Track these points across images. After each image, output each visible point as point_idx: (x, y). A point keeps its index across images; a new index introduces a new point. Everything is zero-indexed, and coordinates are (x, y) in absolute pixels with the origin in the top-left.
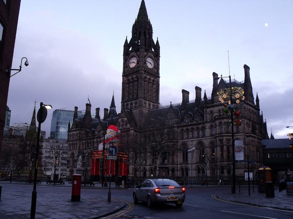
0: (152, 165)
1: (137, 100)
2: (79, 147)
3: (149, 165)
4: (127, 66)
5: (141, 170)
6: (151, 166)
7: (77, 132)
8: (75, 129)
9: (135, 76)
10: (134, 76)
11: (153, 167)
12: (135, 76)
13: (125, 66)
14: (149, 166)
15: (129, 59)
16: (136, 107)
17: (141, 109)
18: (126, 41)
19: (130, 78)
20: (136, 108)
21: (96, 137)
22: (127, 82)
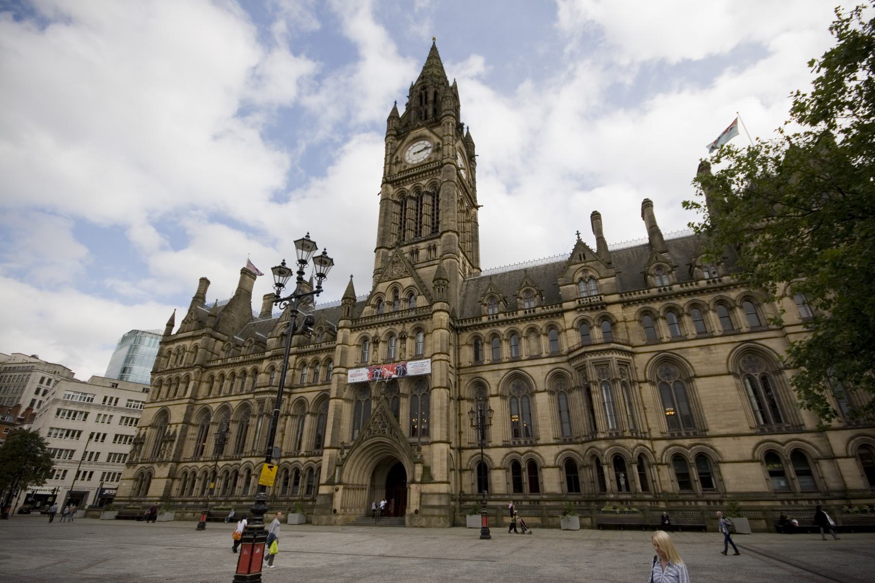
0: (514, 446)
1: (437, 240)
2: (196, 389)
3: (504, 446)
4: (399, 160)
5: (464, 466)
6: (515, 449)
7: (199, 341)
8: (190, 334)
9: (427, 180)
10: (424, 182)
11: (522, 455)
12: (427, 180)
13: (391, 160)
14: (505, 451)
15: (406, 146)
16: (434, 260)
17: (453, 262)
18: (395, 110)
19: (408, 187)
20: (431, 263)
21: (268, 354)
22: (395, 198)
